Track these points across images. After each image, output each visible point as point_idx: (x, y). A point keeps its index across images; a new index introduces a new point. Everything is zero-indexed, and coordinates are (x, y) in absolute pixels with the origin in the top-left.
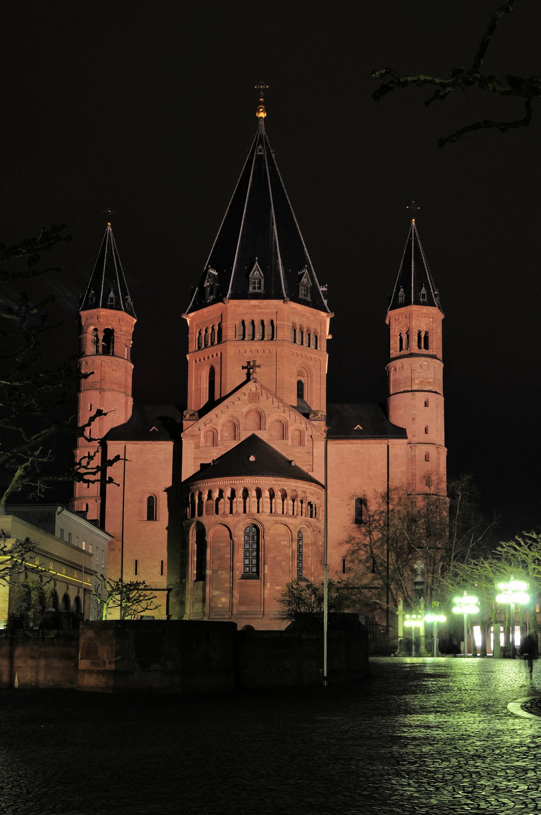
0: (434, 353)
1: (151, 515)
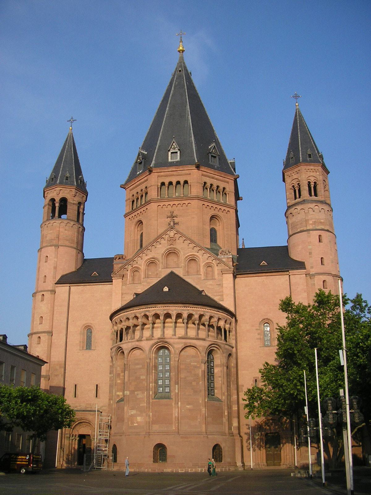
0: (323, 199)
1: (88, 344)
